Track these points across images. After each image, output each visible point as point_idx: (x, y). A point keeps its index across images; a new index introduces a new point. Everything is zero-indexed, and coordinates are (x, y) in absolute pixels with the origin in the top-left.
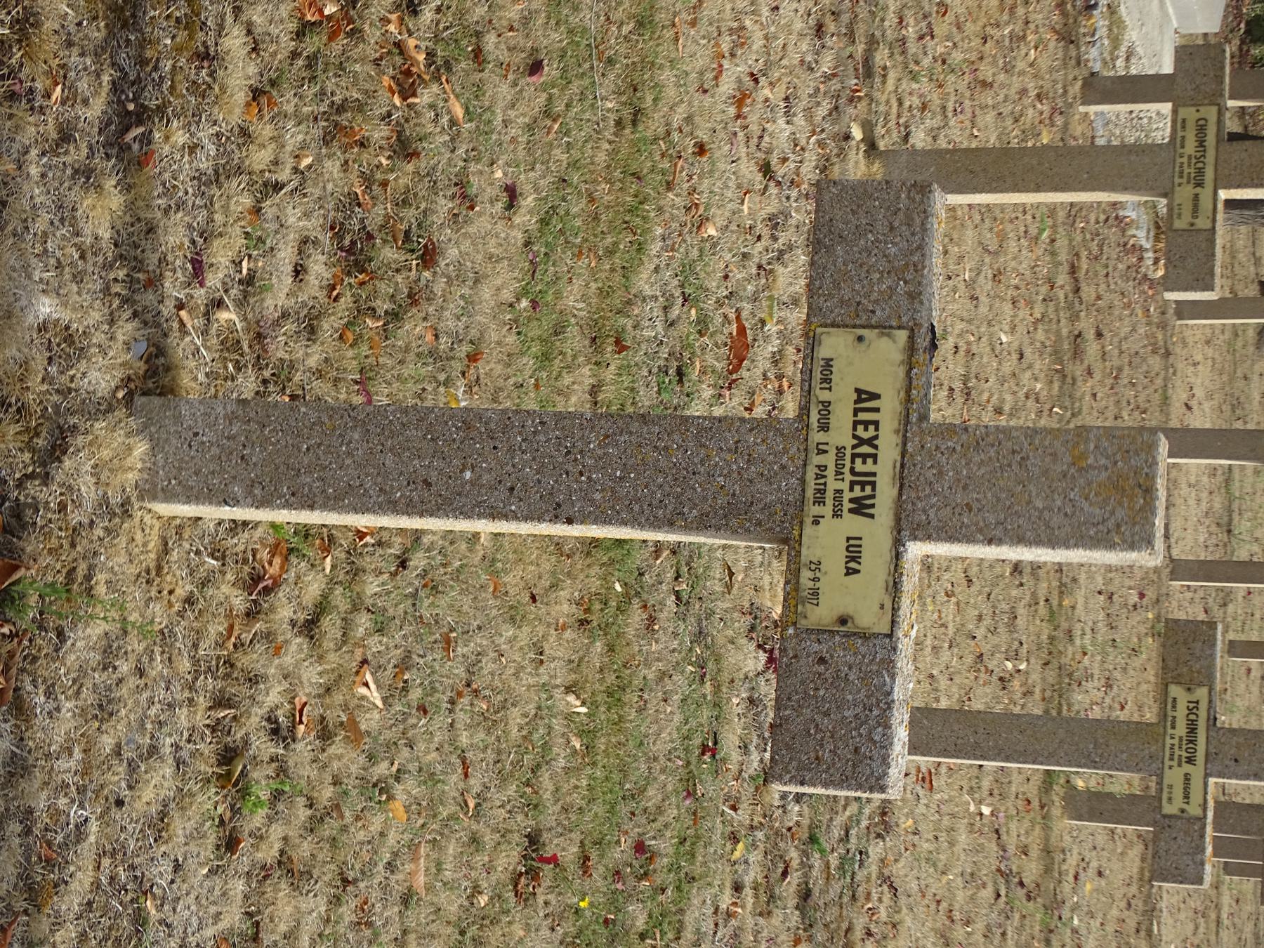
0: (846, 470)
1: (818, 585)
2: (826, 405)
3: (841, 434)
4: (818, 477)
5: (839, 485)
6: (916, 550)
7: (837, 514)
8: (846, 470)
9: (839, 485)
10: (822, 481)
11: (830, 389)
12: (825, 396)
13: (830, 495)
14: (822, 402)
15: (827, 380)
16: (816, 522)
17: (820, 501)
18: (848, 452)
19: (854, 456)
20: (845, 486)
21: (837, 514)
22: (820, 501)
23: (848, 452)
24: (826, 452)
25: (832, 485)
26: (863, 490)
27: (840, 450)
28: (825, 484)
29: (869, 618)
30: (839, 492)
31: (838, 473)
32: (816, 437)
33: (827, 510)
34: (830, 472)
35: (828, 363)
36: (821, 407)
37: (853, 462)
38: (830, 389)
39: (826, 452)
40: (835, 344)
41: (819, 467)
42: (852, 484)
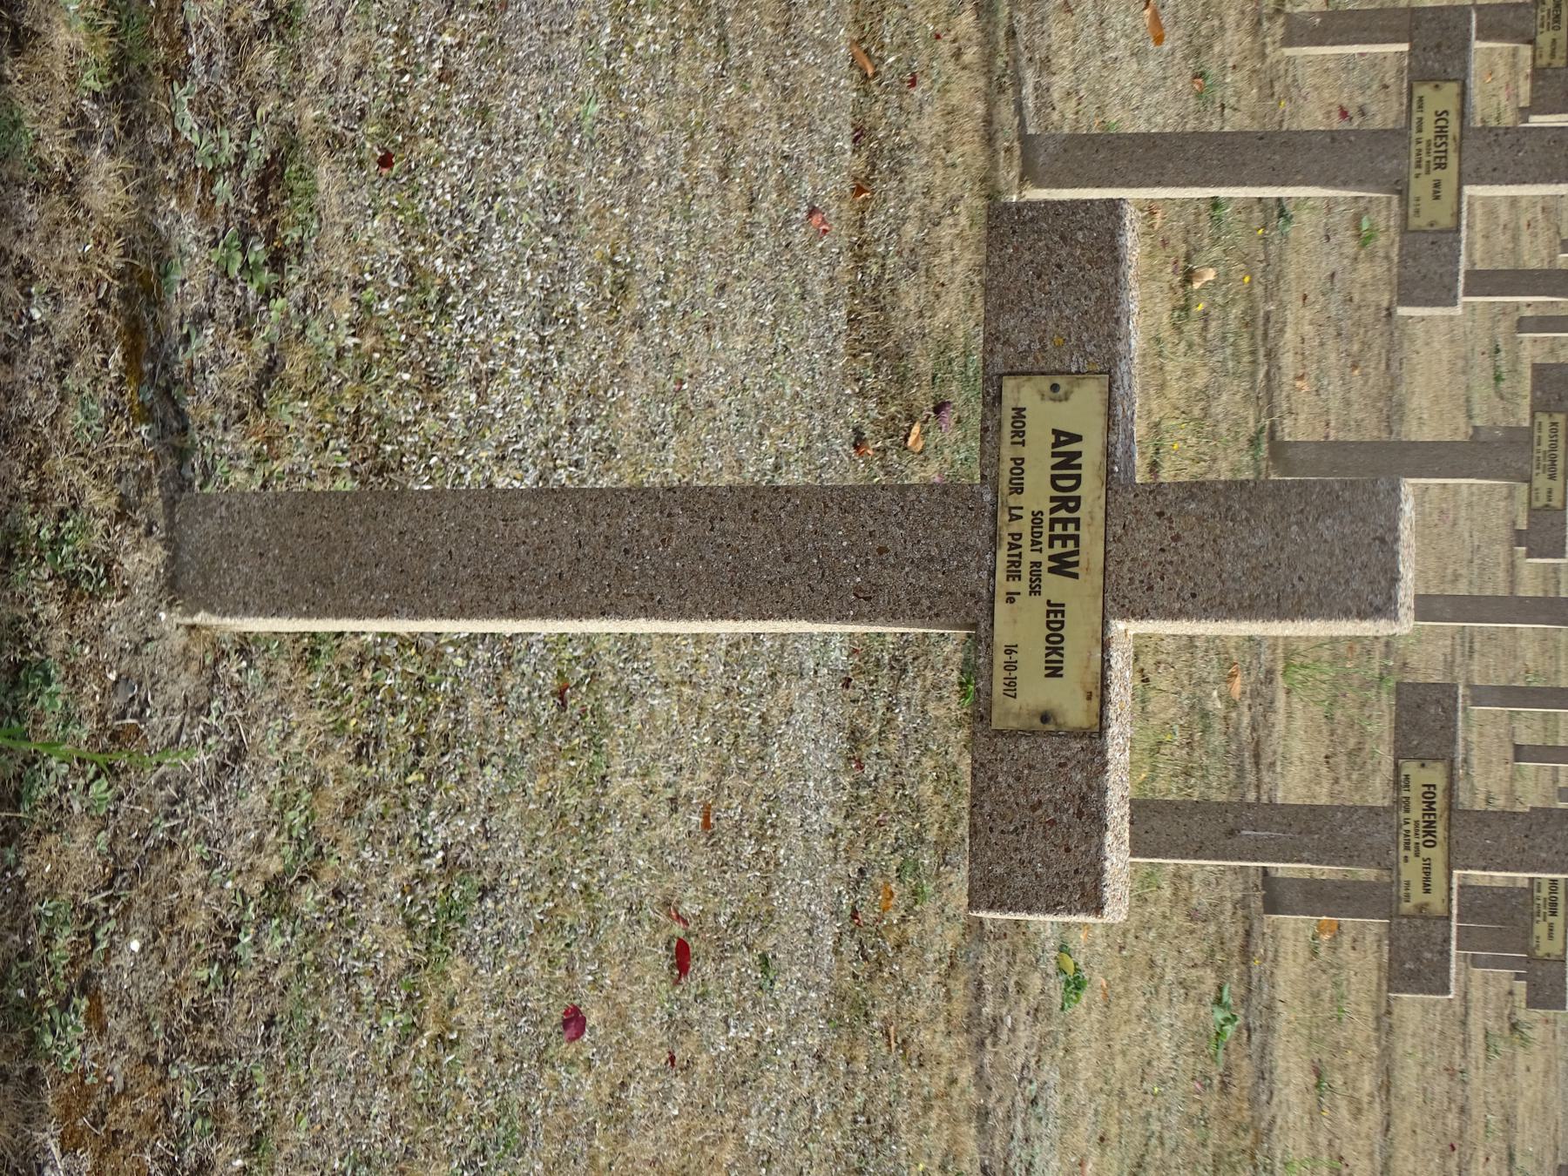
0: (1045, 539)
1: (1014, 674)
4: (1012, 546)
7: (1035, 590)
9: (1036, 557)
11: (1023, 443)
13: (1025, 570)
16: (1011, 600)
18: (1046, 518)
19: (1053, 522)
20: (1043, 558)
23: (1046, 518)
25: (1028, 556)
27: (1037, 517)
28: (1020, 555)
29: (1076, 713)
30: (1036, 564)
31: (1034, 543)
33: (1023, 586)
34: (1026, 541)
37: (1052, 529)
38: (1023, 443)
40: (1023, 393)
41: (1012, 535)
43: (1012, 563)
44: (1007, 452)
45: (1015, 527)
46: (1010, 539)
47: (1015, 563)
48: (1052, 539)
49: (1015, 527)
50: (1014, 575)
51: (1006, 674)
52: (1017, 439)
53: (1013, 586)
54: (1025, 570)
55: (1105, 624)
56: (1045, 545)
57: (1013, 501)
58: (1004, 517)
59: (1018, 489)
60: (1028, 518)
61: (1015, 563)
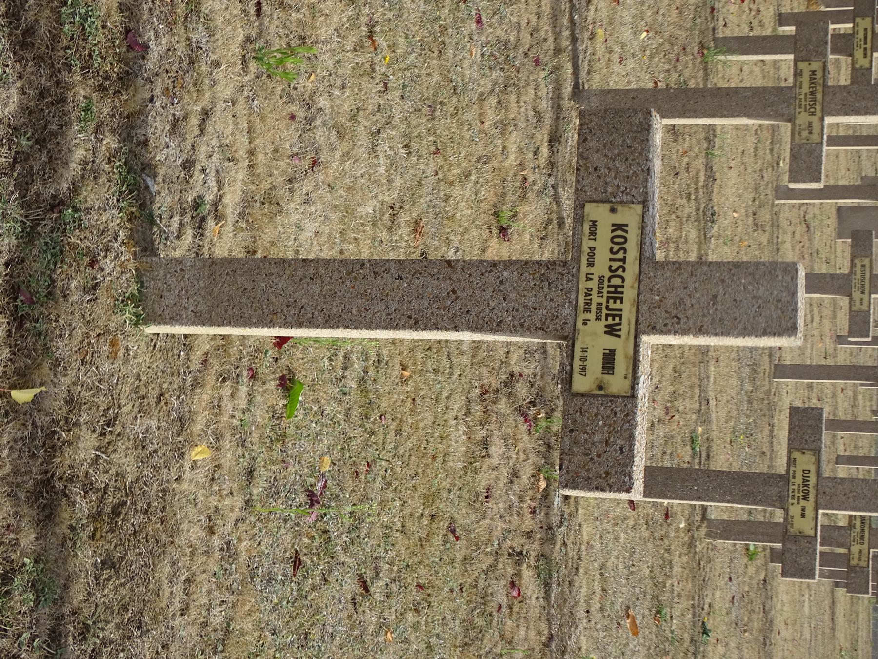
1: (585, 363)
2: (592, 249)
3: (601, 267)
4: (587, 295)
6: (649, 340)
7: (598, 318)
8: (606, 289)
9: (600, 300)
10: (589, 298)
11: (595, 239)
12: (592, 244)
13: (593, 307)
14: (590, 248)
15: (593, 234)
16: (585, 323)
17: (587, 310)
18: (606, 279)
22: (587, 310)
24: (592, 279)
25: (595, 299)
27: (601, 279)
28: (591, 300)
29: (617, 383)
30: (600, 304)
31: (599, 293)
32: (584, 269)
33: (591, 316)
34: (594, 292)
35: (594, 223)
36: (589, 251)
38: (595, 239)
39: (592, 279)
40: (597, 212)
41: (587, 289)
42: (608, 299)
43: (586, 304)
44: (587, 244)
45: (590, 284)
46: (586, 291)
47: (588, 304)
49: (590, 284)
51: (581, 363)
52: (592, 237)
53: (587, 316)
54: (593, 307)
55: (636, 336)
57: (592, 270)
58: (583, 277)
59: (591, 264)
60: (596, 278)
61: (588, 304)
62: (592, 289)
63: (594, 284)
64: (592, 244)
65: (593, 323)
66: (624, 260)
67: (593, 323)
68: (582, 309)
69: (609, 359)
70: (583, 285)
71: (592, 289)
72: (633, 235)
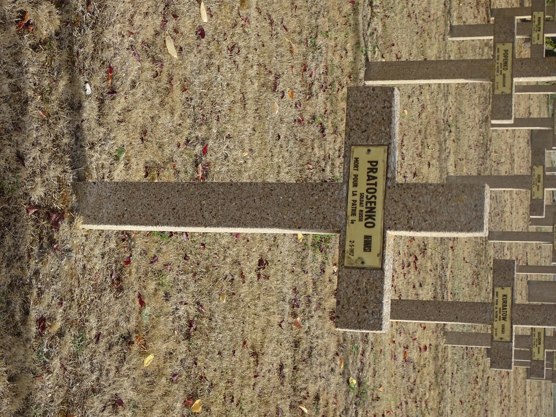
0: (364, 203)
2: (356, 176)
3: (362, 187)
4: (353, 205)
5: (361, 208)
7: (360, 220)
8: (364, 203)
9: (361, 208)
11: (358, 170)
12: (355, 172)
13: (357, 212)
14: (354, 175)
15: (356, 166)
16: (352, 222)
21: (360, 220)
25: (359, 208)
26: (371, 205)
28: (356, 207)
30: (361, 211)
31: (361, 204)
32: (351, 189)
33: (357, 218)
34: (358, 203)
36: (354, 177)
38: (358, 170)
39: (356, 195)
41: (353, 201)
43: (353, 210)
44: (353, 172)
46: (352, 202)
48: (367, 203)
50: (354, 214)
56: (364, 205)
57: (355, 189)
58: (350, 194)
59: (355, 185)
60: (359, 195)
62: (356, 201)
63: (357, 198)
64: (355, 172)
65: (357, 222)
66: (376, 184)
67: (357, 222)
68: (351, 214)
69: (368, 244)
70: (351, 198)
71: (356, 201)
72: (381, 167)
